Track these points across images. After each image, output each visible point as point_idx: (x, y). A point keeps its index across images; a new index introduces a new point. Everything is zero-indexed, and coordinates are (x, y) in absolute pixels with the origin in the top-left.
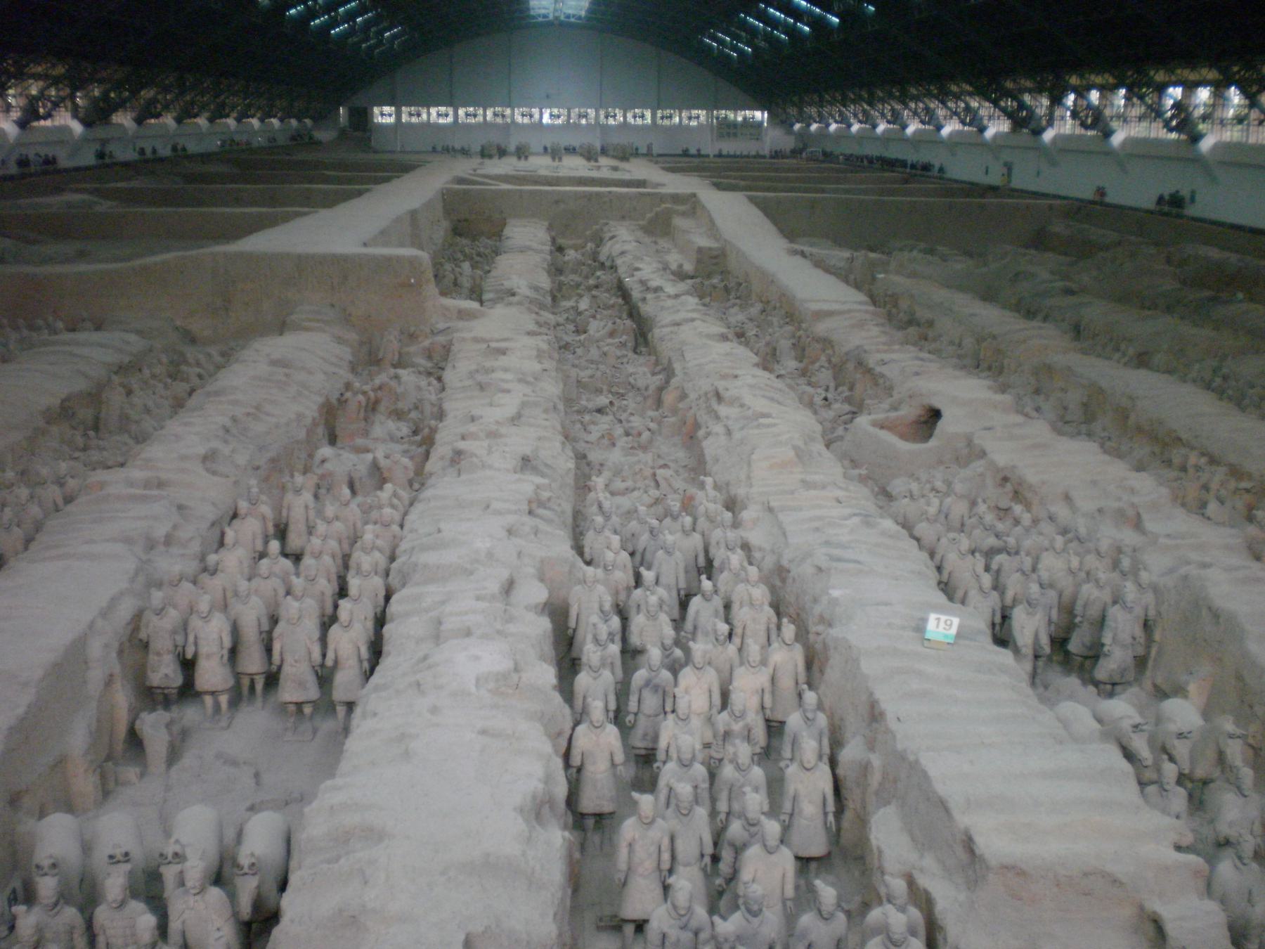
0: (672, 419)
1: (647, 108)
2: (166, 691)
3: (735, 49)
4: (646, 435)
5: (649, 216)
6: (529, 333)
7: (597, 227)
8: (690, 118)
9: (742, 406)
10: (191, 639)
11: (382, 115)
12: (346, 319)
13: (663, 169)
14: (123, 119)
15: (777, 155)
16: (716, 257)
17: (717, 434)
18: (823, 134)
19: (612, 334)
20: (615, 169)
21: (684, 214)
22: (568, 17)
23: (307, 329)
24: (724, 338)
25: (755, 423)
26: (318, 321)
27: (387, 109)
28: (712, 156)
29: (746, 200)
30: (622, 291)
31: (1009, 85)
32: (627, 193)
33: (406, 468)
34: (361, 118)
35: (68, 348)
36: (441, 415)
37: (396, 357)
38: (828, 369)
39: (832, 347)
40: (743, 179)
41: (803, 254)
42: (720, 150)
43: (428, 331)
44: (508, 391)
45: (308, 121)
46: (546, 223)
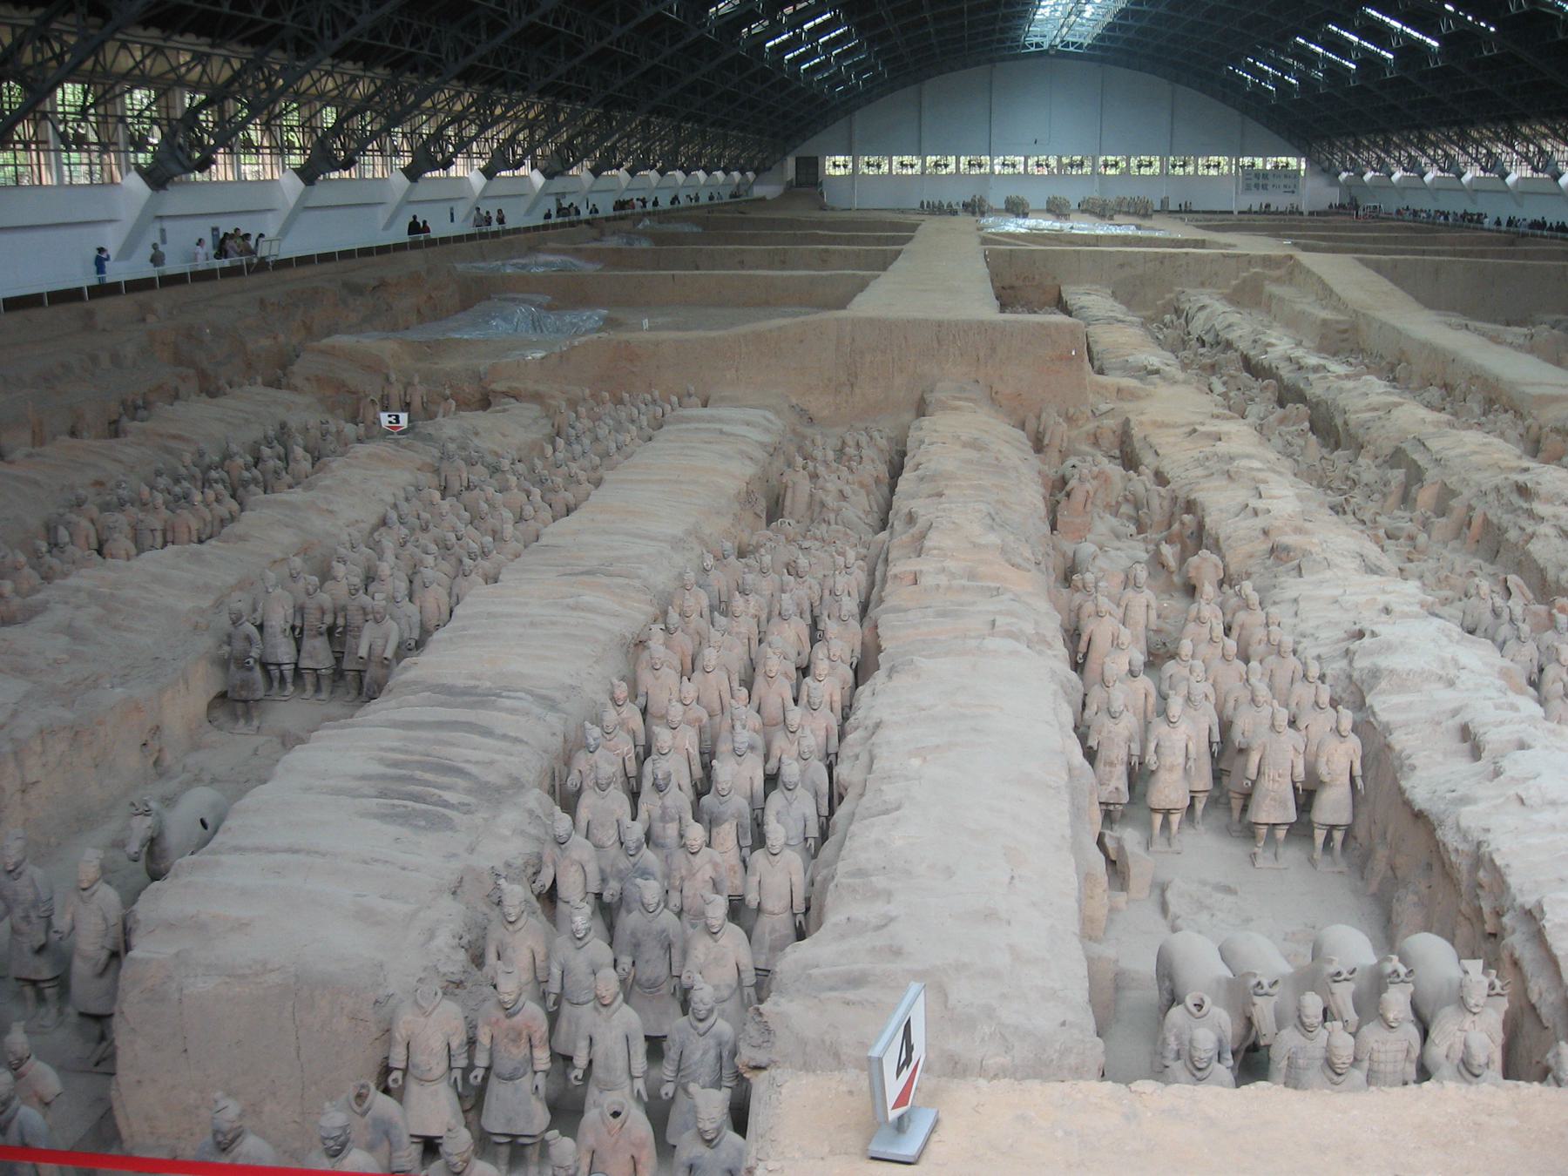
0: (1443, 520)
2: (1111, 808)
3: (1277, 81)
4: (1422, 538)
5: (1234, 282)
7: (1172, 295)
8: (1218, 166)
10: (1152, 746)
11: (835, 165)
12: (994, 400)
13: (1198, 227)
14: (581, 173)
16: (1345, 331)
18: (1384, 185)
19: (1282, 421)
20: (1139, 227)
21: (1277, 281)
22: (1067, 45)
23: (956, 408)
24: (1452, 426)
26: (967, 399)
27: (840, 159)
28: (1236, 213)
29: (1357, 263)
30: (1254, 369)
32: (1208, 255)
33: (1216, 566)
34: (810, 170)
35: (718, 426)
36: (1190, 506)
40: (1323, 238)
42: (1268, 206)
43: (1090, 414)
45: (750, 175)
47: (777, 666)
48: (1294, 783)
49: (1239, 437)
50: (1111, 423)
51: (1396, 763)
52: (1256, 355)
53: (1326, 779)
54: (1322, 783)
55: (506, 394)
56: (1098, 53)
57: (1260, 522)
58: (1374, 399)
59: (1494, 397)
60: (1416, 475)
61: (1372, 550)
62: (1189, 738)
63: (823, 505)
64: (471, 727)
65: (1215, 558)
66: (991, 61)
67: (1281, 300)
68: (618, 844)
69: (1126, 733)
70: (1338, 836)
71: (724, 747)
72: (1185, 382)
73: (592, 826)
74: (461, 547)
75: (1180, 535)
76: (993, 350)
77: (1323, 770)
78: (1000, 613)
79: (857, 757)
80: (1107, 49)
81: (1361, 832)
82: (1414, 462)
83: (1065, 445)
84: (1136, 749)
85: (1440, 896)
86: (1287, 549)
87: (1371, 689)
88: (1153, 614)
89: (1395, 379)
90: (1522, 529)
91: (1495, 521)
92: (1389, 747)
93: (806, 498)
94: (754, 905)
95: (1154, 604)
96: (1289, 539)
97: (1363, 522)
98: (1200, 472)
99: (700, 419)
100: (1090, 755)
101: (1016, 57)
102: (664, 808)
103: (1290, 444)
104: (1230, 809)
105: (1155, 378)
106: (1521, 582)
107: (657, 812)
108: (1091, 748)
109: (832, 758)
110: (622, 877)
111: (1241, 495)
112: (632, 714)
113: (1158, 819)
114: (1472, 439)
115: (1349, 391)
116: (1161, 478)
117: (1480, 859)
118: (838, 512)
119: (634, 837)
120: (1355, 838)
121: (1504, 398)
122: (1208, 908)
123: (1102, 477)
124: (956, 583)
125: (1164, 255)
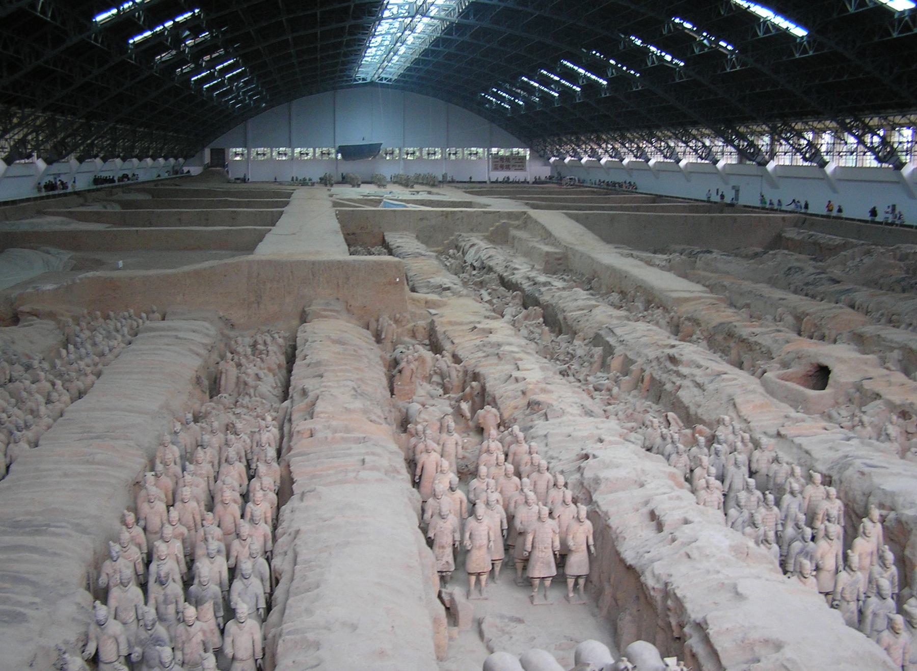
1: (459, 148)
2: (444, 574)
3: (510, 102)
4: (615, 390)
5: (492, 229)
6: (487, 317)
9: (699, 366)
10: (467, 535)
13: (466, 192)
15: (537, 182)
16: (559, 259)
17: (688, 387)
18: (577, 165)
20: (430, 193)
21: (517, 227)
22: (381, 80)
23: (326, 317)
24: (628, 319)
25: (719, 378)
26: (331, 311)
27: (239, 150)
29: (563, 215)
31: (742, 129)
32: (475, 212)
33: (496, 416)
34: (219, 157)
35: (174, 333)
36: (476, 377)
37: (395, 337)
38: (703, 340)
39: (699, 324)
41: (632, 255)
42: (508, 178)
44: (521, 359)
46: (415, 236)
47: (230, 495)
48: (554, 552)
49: (502, 330)
50: (422, 323)
51: (614, 536)
52: (507, 276)
53: (573, 548)
54: (570, 551)
55: (30, 314)
56: (401, 84)
57: (521, 386)
58: (580, 303)
59: (650, 298)
60: (609, 350)
61: (588, 402)
62: (490, 528)
63: (246, 384)
64: (33, 549)
65: (494, 410)
66: (334, 89)
67: (520, 239)
68: (136, 621)
69: (451, 527)
70: (582, 582)
71: (200, 552)
72: (467, 296)
73: (119, 610)
74: (10, 422)
75: (471, 394)
76: (348, 279)
77: (571, 543)
78: (367, 454)
79: (286, 553)
80: (406, 82)
81: (595, 578)
82: (608, 342)
83: (395, 337)
84: (457, 537)
85: (645, 617)
86: (538, 403)
87: (596, 490)
88: (460, 448)
89: (591, 288)
90: (674, 383)
91: (658, 378)
92: (609, 527)
93: (234, 380)
94: (230, 655)
95: (460, 443)
96: (541, 397)
97: (579, 381)
98: (480, 354)
99: (163, 329)
100: (430, 543)
101: (351, 86)
102: (166, 595)
103: (532, 332)
104: (516, 569)
105: (448, 293)
106: (675, 416)
107: (161, 598)
108: (430, 538)
109: (269, 554)
110: (141, 643)
111: (508, 368)
112: (138, 531)
113: (473, 578)
114: (641, 326)
115: (566, 298)
116: (457, 359)
117: (667, 593)
118: (255, 388)
119: (151, 618)
120: (591, 582)
121: (657, 300)
122: (507, 633)
123: (421, 360)
124: (338, 435)
125: (447, 213)
